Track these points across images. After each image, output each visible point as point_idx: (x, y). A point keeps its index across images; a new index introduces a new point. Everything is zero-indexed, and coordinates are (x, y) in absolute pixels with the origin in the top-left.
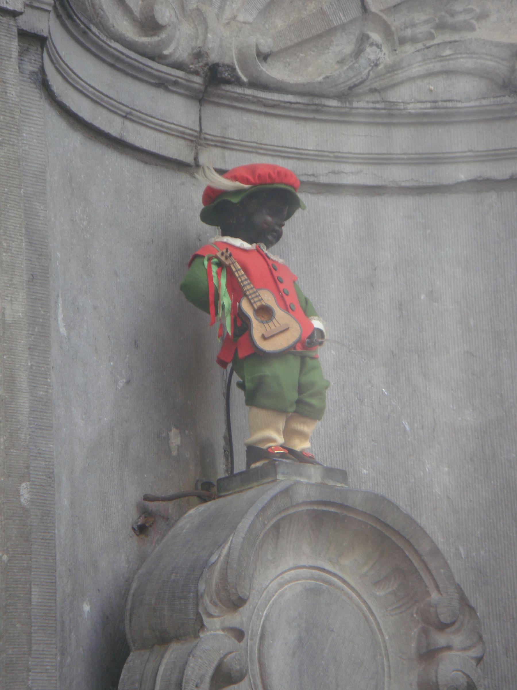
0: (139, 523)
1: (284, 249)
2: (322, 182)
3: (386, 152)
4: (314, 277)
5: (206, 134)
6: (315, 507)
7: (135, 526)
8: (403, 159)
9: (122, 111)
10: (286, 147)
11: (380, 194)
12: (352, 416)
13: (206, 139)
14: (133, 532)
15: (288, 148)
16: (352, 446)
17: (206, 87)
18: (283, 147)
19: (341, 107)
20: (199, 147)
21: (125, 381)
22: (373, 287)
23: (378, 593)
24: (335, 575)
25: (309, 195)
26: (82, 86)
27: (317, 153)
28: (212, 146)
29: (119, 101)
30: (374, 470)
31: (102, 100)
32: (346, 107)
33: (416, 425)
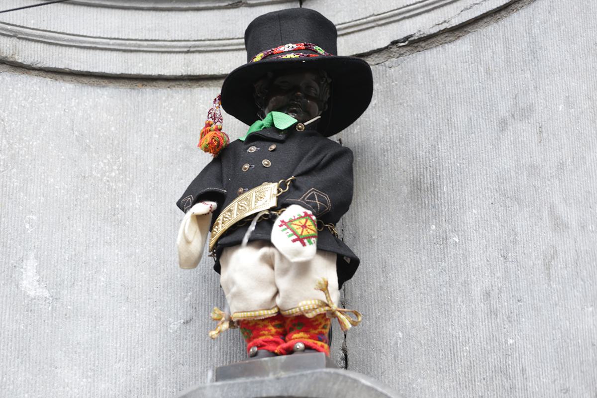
1: (419, 115)
4: (452, 134)
9: (180, 47)
10: (408, 6)
15: (410, 5)
16: (497, 315)
18: (404, 7)
21: (182, 321)
22: (514, 118)
25: (446, 45)
26: (103, 44)
29: (170, 39)
31: (140, 46)
33: (559, 266)
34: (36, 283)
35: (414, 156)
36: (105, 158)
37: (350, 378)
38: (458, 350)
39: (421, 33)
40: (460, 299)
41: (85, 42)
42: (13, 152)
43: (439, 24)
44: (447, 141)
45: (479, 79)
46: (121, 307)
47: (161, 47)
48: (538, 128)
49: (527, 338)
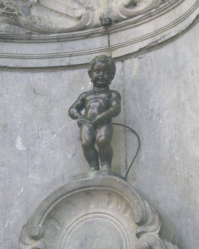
5: (112, 46)
11: (178, 38)
13: (113, 47)
17: (106, 28)
18: (143, 36)
19: (157, 10)
21: (72, 155)
23: (126, 216)
24: (104, 213)
27: (155, 32)
31: (54, 56)
32: (158, 10)
34: (21, 145)
36: (43, 98)
37: (113, 179)
40: (162, 144)
41: (34, 56)
42: (11, 99)
46: (51, 151)
47: (60, 55)
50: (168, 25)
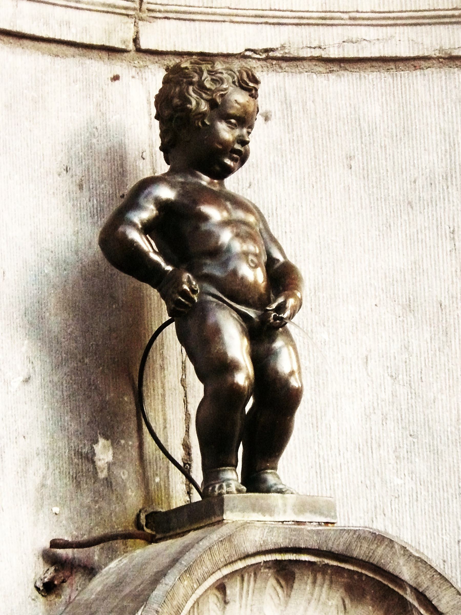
0: (46, 580)
2: (332, 56)
3: (427, 8)
4: (321, 198)
5: (148, 3)
6: (279, 557)
7: (40, 584)
8: (453, 16)
10: (275, 10)
12: (379, 402)
13: (149, 10)
14: (36, 593)
15: (279, 10)
20: (140, 23)
22: (412, 208)
25: (314, 76)
27: (323, 15)
28: (160, 18)
30: (412, 479)
35: (270, 212)
38: (327, 475)
39: (287, 51)
43: (310, 47)
44: (314, 205)
45: (361, 137)
48: (448, 232)
49: (422, 483)
50: (390, 12)
